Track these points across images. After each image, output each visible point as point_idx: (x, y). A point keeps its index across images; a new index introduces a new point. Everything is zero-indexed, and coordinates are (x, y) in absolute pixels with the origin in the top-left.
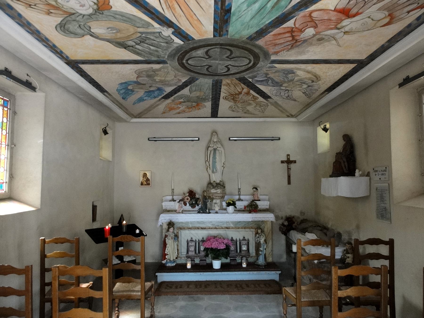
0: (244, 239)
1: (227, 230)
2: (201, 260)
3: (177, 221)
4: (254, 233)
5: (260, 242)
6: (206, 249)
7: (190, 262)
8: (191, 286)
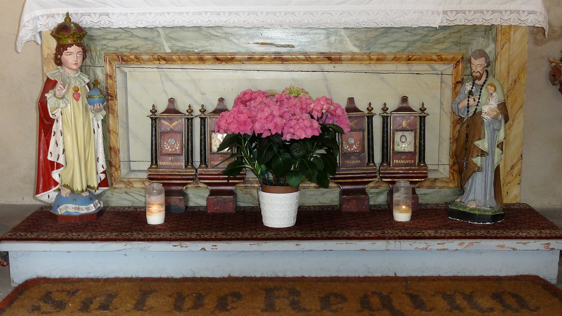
0: (404, 107)
1: (328, 66)
2: (213, 193)
3: (104, 22)
4: (449, 81)
5: (477, 114)
6: (232, 140)
7: (161, 198)
8: (151, 301)
